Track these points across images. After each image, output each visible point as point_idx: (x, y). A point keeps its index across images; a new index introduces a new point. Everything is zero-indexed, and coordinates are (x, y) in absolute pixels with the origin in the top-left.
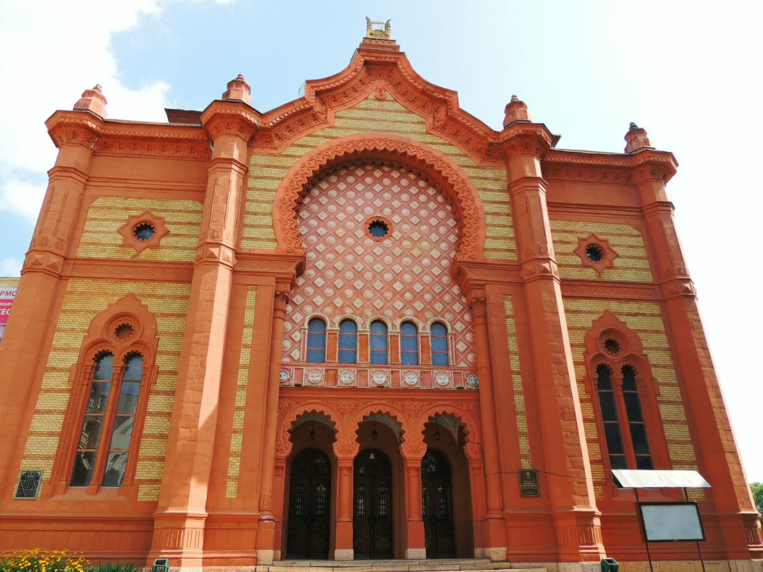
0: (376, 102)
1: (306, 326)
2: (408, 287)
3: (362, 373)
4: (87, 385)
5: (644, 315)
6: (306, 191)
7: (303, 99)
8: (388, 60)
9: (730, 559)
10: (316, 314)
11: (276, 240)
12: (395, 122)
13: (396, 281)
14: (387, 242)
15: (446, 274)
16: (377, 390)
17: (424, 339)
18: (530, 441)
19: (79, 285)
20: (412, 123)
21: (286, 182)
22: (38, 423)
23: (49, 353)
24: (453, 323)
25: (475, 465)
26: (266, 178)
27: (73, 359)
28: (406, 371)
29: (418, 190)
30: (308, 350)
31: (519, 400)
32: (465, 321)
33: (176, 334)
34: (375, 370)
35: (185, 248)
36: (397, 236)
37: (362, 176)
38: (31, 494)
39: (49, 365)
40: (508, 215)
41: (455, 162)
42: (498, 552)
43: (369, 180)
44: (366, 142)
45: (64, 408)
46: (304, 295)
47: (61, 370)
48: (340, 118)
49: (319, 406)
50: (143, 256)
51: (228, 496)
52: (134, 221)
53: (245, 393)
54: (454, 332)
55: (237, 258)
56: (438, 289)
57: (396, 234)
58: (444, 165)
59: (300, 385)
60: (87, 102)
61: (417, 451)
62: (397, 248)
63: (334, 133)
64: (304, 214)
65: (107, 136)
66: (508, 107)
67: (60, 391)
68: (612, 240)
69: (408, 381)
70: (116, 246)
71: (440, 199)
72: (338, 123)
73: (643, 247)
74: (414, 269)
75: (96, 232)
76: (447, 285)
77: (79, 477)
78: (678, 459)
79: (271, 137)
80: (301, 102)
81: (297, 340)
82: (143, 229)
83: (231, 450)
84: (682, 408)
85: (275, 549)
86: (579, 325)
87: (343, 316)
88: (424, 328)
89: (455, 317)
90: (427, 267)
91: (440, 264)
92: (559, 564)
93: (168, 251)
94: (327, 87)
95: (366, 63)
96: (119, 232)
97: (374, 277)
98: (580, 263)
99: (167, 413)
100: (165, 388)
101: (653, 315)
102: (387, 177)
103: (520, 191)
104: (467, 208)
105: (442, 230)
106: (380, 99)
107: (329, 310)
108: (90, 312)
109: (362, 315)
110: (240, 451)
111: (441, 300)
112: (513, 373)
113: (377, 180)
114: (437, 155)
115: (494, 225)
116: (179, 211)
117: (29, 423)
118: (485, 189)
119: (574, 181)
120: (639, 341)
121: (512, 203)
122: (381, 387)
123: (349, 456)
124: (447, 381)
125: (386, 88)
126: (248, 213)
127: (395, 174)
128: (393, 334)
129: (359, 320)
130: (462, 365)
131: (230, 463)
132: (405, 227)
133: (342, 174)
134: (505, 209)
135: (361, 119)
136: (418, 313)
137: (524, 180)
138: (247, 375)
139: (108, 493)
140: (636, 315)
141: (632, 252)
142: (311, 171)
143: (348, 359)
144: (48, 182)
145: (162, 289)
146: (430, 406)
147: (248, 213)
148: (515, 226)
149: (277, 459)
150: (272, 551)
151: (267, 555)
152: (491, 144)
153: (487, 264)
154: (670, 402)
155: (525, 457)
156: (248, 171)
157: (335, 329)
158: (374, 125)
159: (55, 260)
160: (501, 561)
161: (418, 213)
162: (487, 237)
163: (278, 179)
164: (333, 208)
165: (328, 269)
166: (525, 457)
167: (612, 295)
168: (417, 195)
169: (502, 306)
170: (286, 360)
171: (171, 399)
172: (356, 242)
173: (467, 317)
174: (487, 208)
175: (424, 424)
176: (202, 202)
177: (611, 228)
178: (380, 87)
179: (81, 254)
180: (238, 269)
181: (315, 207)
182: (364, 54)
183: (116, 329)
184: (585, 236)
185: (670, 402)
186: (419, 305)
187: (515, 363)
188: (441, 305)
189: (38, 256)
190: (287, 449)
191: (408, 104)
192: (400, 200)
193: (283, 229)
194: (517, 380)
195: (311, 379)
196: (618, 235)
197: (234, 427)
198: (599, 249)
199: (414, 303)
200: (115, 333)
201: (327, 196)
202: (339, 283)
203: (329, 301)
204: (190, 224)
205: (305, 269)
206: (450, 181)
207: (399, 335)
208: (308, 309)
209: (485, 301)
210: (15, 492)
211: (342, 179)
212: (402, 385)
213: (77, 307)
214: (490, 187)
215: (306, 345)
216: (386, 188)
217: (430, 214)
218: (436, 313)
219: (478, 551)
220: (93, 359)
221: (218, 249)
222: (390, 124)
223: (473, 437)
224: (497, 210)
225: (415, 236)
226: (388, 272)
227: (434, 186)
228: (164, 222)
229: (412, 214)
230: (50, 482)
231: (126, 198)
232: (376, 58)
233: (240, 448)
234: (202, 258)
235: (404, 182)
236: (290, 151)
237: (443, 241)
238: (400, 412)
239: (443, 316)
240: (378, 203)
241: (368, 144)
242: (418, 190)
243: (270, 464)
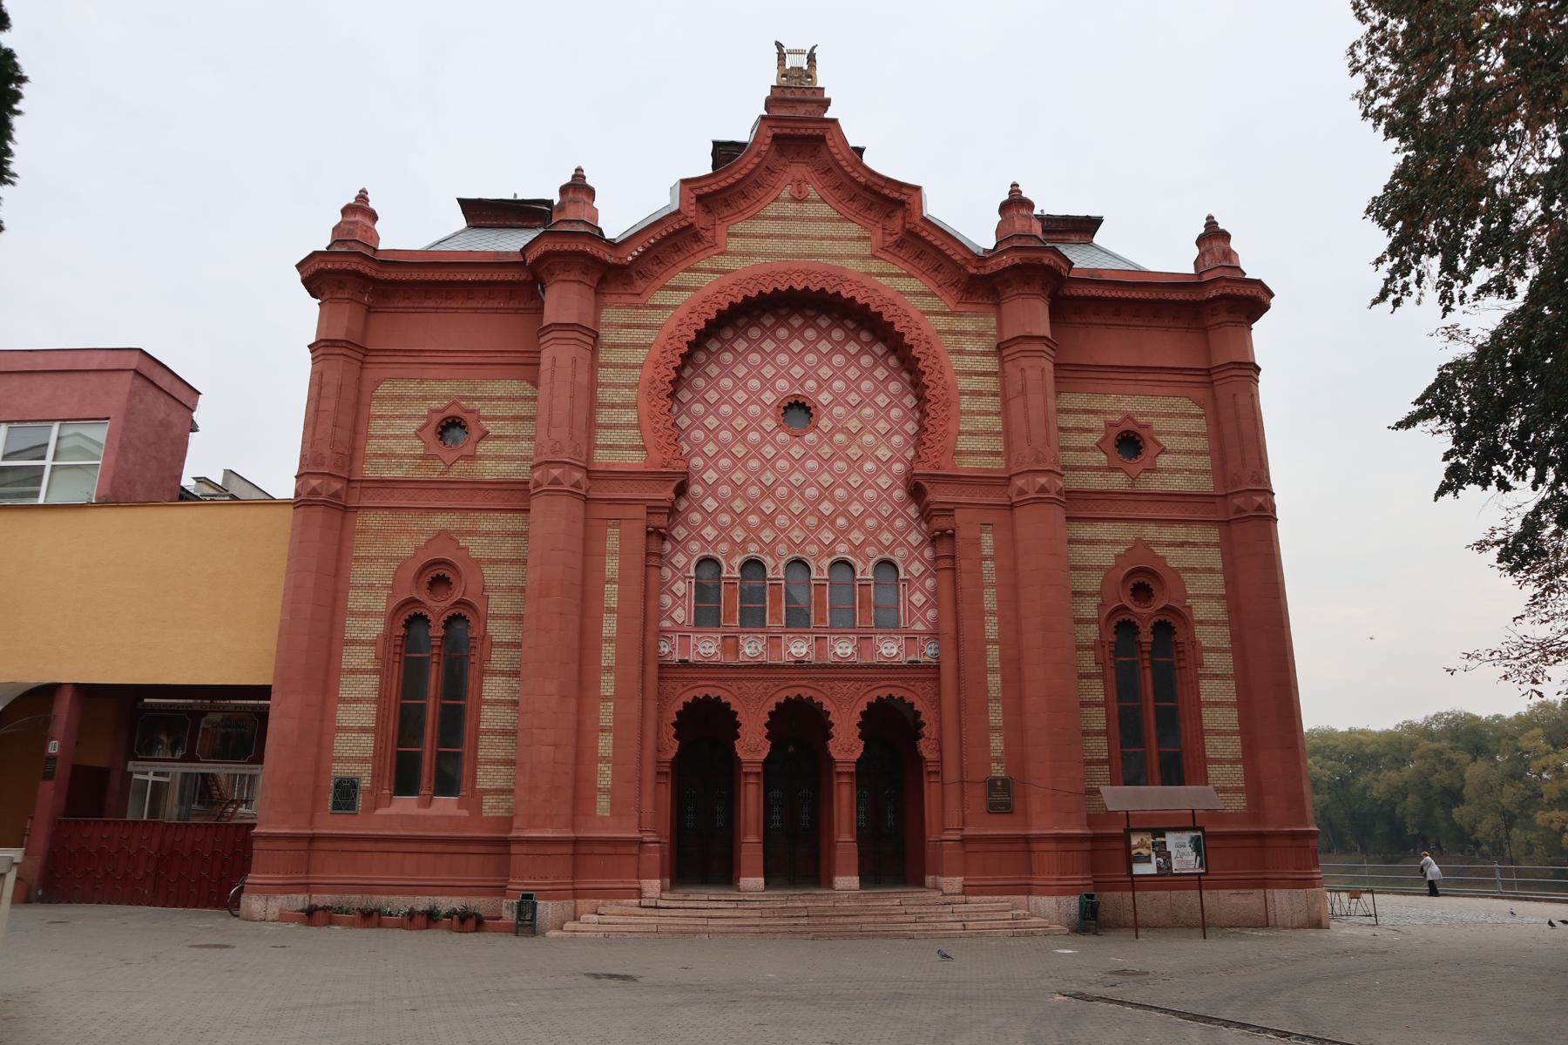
0: (793, 205)
1: (692, 573)
2: (842, 509)
3: (774, 639)
4: (399, 662)
5: (1194, 545)
6: (687, 358)
7: (678, 212)
8: (810, 132)
9: (1267, 888)
10: (706, 554)
11: (644, 448)
12: (822, 239)
13: (823, 500)
14: (810, 437)
15: (899, 487)
16: (795, 667)
17: (864, 589)
18: (1005, 739)
19: (373, 520)
20: (849, 240)
21: (657, 351)
22: (346, 716)
23: (345, 621)
24: (907, 561)
25: (930, 770)
26: (625, 346)
27: (376, 627)
28: (837, 637)
29: (858, 348)
30: (696, 607)
31: (994, 680)
32: (924, 559)
33: (511, 589)
34: (791, 636)
35: (511, 459)
36: (826, 426)
37: (772, 326)
38: (351, 806)
39: (347, 636)
40: (995, 395)
41: (917, 305)
42: (953, 883)
43: (782, 333)
44: (777, 278)
45: (375, 694)
46: (687, 523)
47: (363, 643)
48: (735, 235)
49: (714, 689)
50: (453, 475)
51: (599, 813)
52: (441, 416)
53: (612, 678)
54: (908, 577)
55: (589, 478)
56: (886, 510)
57: (825, 424)
58: (899, 312)
59: (687, 661)
60: (352, 227)
61: (850, 750)
62: (825, 445)
63: (726, 263)
64: (685, 395)
65: (386, 282)
66: (1004, 208)
67: (366, 672)
68: (1158, 424)
69: (839, 651)
70: (415, 458)
71: (892, 361)
72: (733, 244)
73: (1204, 435)
74: (851, 481)
75: (385, 437)
76: (900, 505)
77: (405, 783)
78: (1217, 756)
79: (630, 277)
80: (674, 219)
81: (680, 594)
82: (449, 426)
83: (600, 755)
84: (1233, 684)
85: (661, 877)
86: (1094, 562)
87: (746, 555)
88: (865, 571)
89: (911, 554)
90: (870, 476)
91: (890, 469)
92: (1031, 897)
93: (489, 464)
94: (715, 187)
95: (775, 137)
96: (417, 436)
97: (791, 494)
98: (1105, 463)
99: (509, 701)
100: (504, 667)
101: (1208, 545)
102: (811, 326)
103: (1013, 357)
104: (931, 385)
105: (895, 413)
106: (799, 200)
107: (724, 547)
108: (391, 559)
109: (772, 554)
110: (611, 755)
111: (891, 528)
112: (988, 642)
113: (796, 333)
114: (888, 296)
115: (973, 413)
116: (500, 399)
117: (334, 715)
118: (961, 352)
119: (1105, 325)
120: (1182, 586)
121: (1001, 374)
122: (800, 665)
123: (757, 758)
124: (895, 651)
125: (809, 180)
126: (602, 405)
127: (824, 322)
128: (818, 583)
129: (769, 561)
130: (919, 627)
131: (599, 772)
132: (838, 410)
133: (741, 325)
134: (990, 384)
135: (768, 236)
136: (856, 549)
137: (1020, 340)
138: (614, 652)
139: (446, 805)
140: (1182, 544)
141: (1187, 444)
142: (693, 331)
143: (753, 618)
144: (310, 362)
145: (486, 523)
146: (869, 688)
147: (602, 405)
148: (1004, 413)
149: (659, 762)
150: (659, 881)
151: (652, 886)
152: (972, 276)
153: (959, 476)
154: (1216, 676)
155: (998, 760)
156: (598, 336)
157: (735, 576)
158: (789, 247)
159: (337, 485)
160: (955, 894)
161: (858, 387)
162: (960, 433)
164: (727, 383)
165: (722, 484)
166: (998, 760)
167: (1149, 515)
168: (857, 355)
169: (977, 542)
170: (666, 624)
171: (513, 682)
172: (763, 438)
173: (928, 553)
174: (964, 383)
175: (861, 713)
176: (535, 384)
177: (1158, 404)
178: (799, 176)
179: (370, 474)
180: (592, 495)
181: (700, 382)
182: (773, 124)
183: (429, 583)
184: (1116, 418)
185: (1216, 676)
186: (857, 537)
187: (991, 629)
188: (891, 538)
189: (314, 482)
190: (672, 748)
191: (841, 207)
192: (830, 365)
193: (657, 430)
194: (993, 652)
195: (702, 651)
196: (1169, 415)
197: (601, 724)
198: (1137, 438)
199: (849, 533)
200: (428, 588)
201: (718, 363)
202: (738, 505)
203: (724, 533)
204: (517, 418)
205: (688, 484)
206: (907, 340)
207: (828, 583)
208: (695, 546)
209: (952, 536)
210: (330, 804)
211: (741, 332)
212: (831, 659)
213: (373, 553)
214: (969, 347)
215: (693, 602)
216: (810, 346)
217: (876, 387)
218: (882, 547)
219: (929, 879)
220: (403, 626)
221: (561, 470)
222: (816, 243)
223: (929, 730)
224: (977, 387)
225: (853, 425)
226: (811, 485)
227: (884, 341)
228: (480, 418)
229: (848, 389)
230: (370, 791)
231: (422, 381)
232: (792, 129)
234: (541, 485)
235: (837, 335)
236: (659, 298)
237: (897, 432)
238: (828, 697)
239: (892, 553)
240: (797, 371)
241: (780, 280)
242: (858, 348)
243: (649, 770)
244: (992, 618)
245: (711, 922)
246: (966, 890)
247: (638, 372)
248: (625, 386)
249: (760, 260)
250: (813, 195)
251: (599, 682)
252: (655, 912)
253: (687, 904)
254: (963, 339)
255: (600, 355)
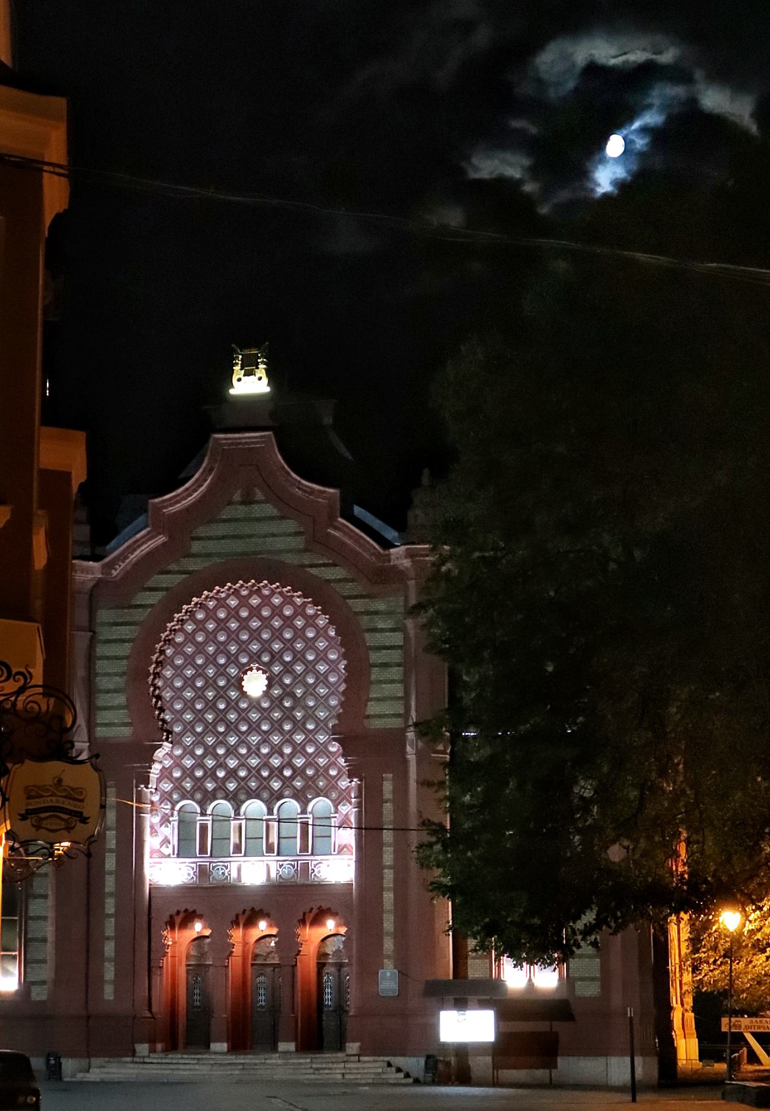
0: (242, 508)
40: (399, 665)
51: (106, 997)
53: (113, 901)
72: (196, 547)
85: (152, 1041)
106: (248, 501)
115: (380, 682)
118: (375, 630)
126: (100, 691)
135: (223, 537)
147: (100, 691)
151: (143, 1048)
158: (238, 546)
163: (128, 641)
166: (389, 957)
174: (374, 657)
214: (381, 625)
233: (113, 954)
244: (389, 848)
245: (175, 1072)
246: (362, 1052)
247: (125, 662)
248: (116, 674)
249: (217, 560)
250: (259, 495)
251: (103, 903)
252: (141, 1066)
253: (164, 1061)
254: (376, 618)
255: (98, 650)
